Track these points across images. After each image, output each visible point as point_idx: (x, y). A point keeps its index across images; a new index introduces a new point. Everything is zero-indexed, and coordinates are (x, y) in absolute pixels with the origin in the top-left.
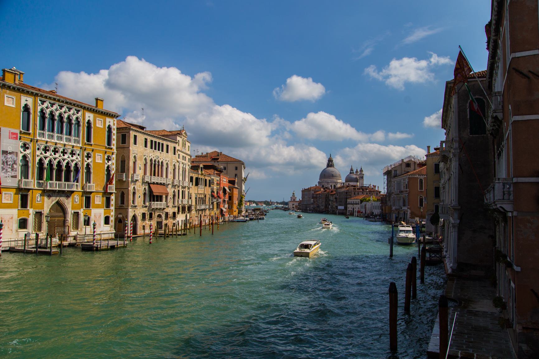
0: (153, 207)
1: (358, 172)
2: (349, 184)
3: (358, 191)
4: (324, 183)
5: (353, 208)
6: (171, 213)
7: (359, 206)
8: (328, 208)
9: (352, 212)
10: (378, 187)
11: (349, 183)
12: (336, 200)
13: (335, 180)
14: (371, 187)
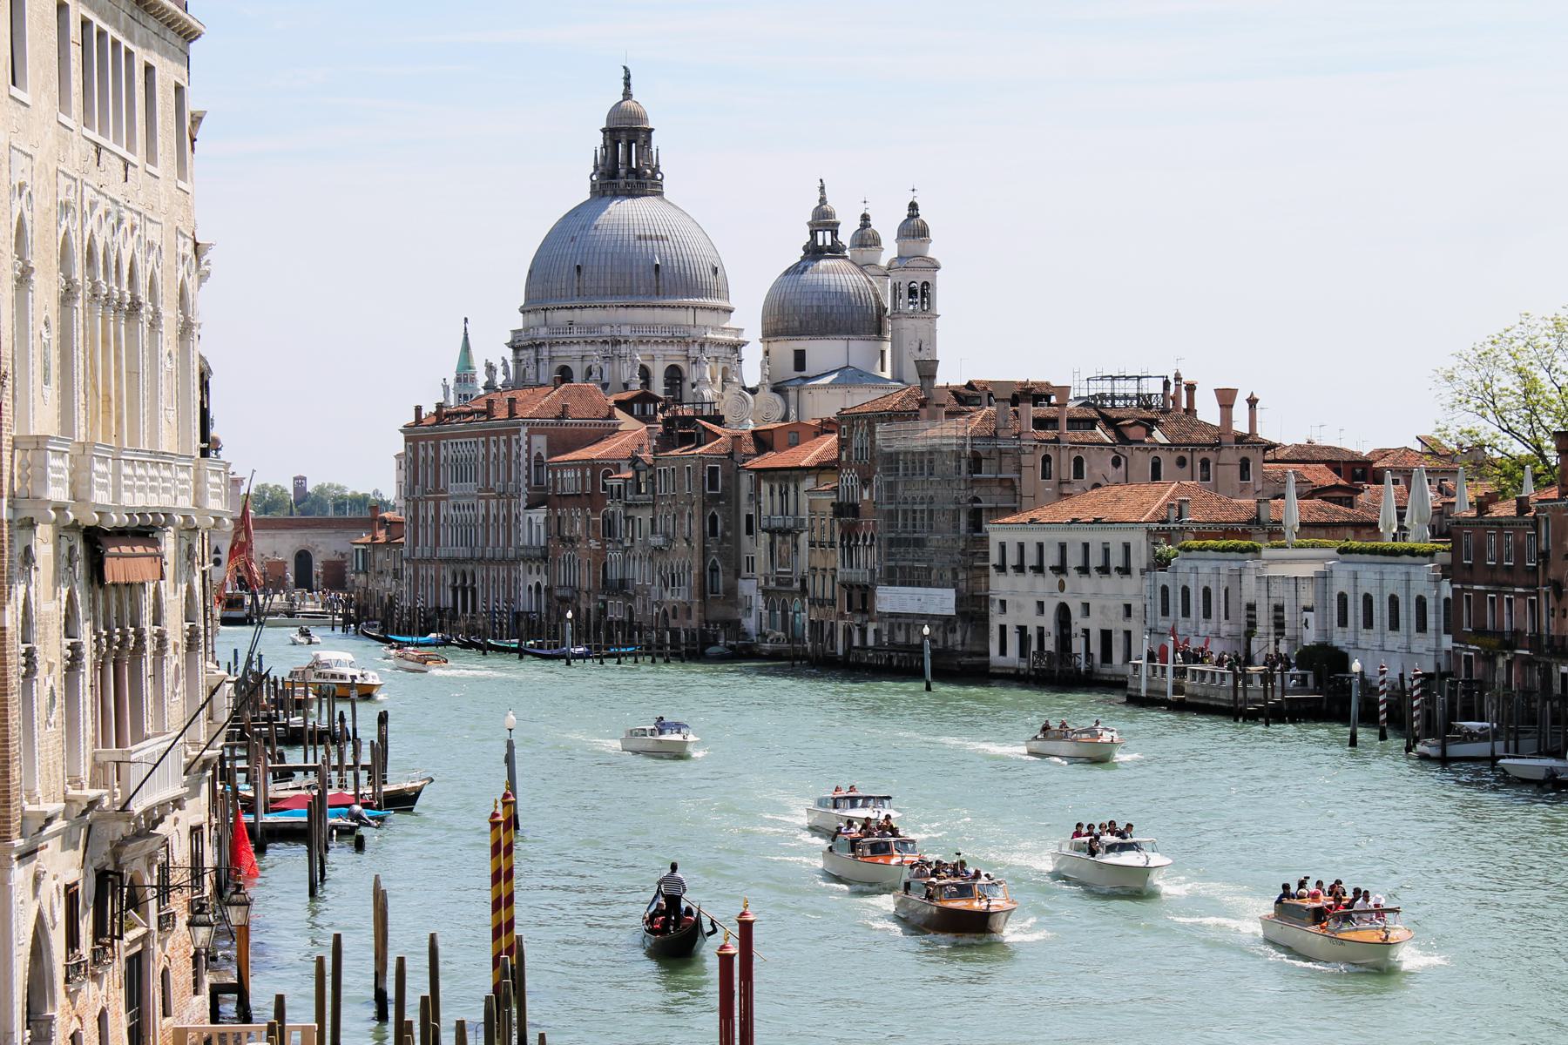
0: (137, 807)
1: (876, 242)
2: (800, 359)
3: (1076, 445)
4: (575, 350)
5: (1063, 612)
6: (181, 853)
7: (1133, 588)
8: (731, 592)
9: (1050, 645)
10: (1252, 402)
11: (799, 345)
12: (849, 533)
13: (684, 317)
14: (1176, 399)
